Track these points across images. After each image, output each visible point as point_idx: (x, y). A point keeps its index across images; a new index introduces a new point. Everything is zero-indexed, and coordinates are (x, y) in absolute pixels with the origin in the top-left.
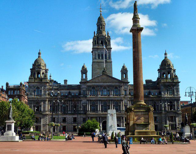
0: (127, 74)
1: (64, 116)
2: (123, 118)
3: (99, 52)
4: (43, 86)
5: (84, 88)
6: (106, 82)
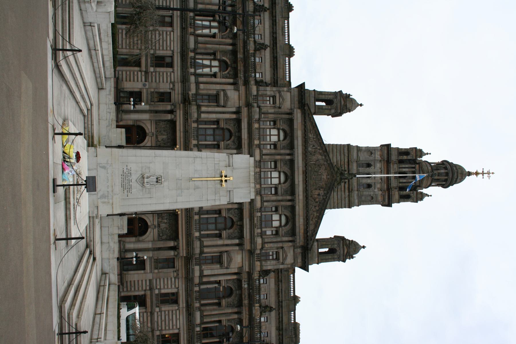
0: (333, 260)
2: (174, 248)
3: (378, 165)
5: (283, 99)
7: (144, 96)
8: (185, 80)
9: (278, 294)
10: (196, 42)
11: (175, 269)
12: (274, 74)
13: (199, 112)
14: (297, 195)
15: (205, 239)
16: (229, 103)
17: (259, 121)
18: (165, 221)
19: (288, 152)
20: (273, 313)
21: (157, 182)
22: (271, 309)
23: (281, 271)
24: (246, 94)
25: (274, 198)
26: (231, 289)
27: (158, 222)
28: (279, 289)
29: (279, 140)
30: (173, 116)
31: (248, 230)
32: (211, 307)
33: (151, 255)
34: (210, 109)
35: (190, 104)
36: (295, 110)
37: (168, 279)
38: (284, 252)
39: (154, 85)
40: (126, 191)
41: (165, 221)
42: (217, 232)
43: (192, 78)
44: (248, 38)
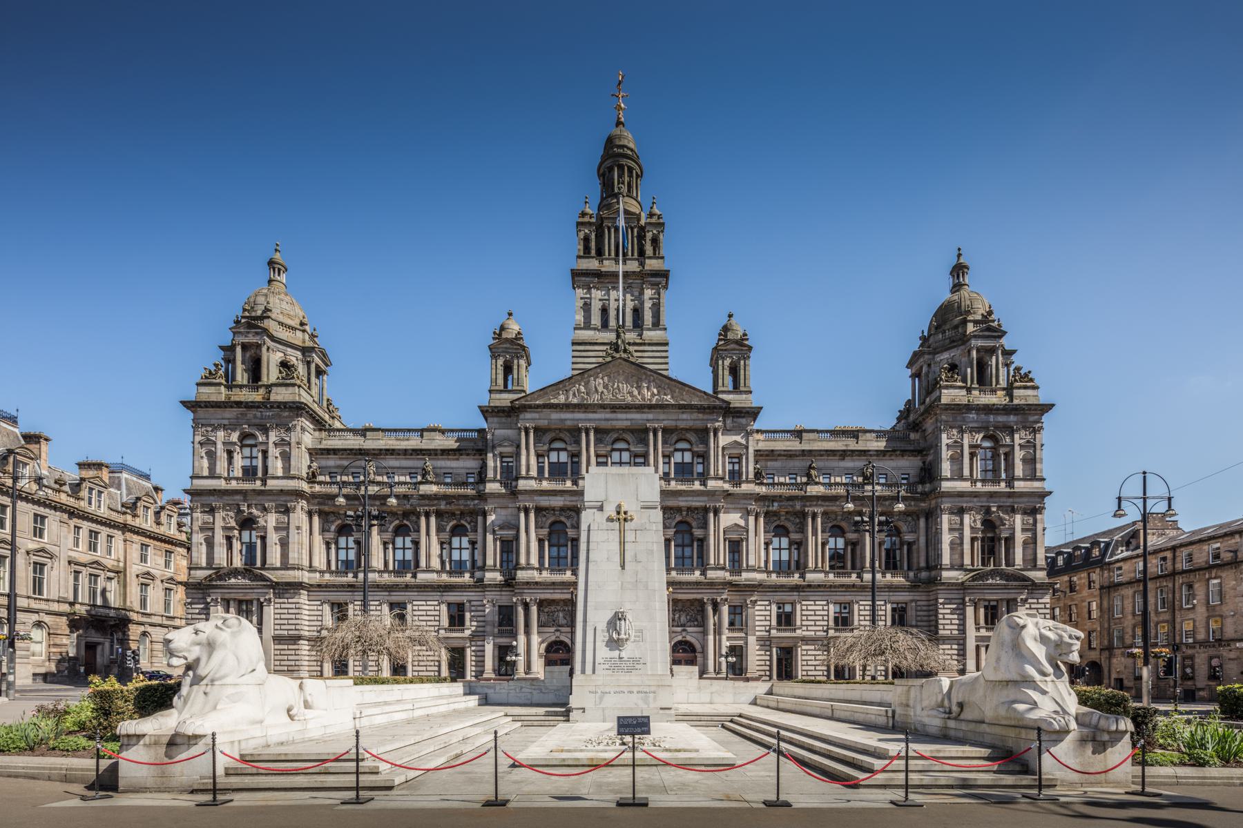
7: (503, 641)
29: (565, 449)
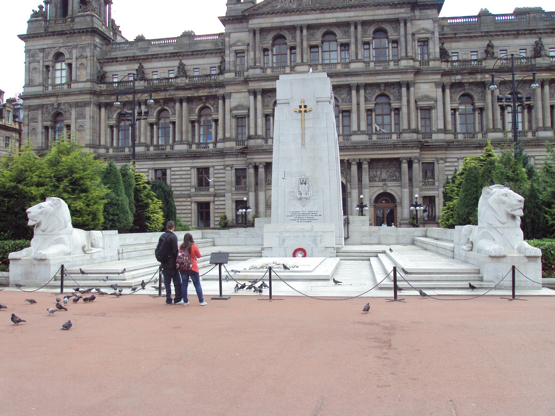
1: (161, 164)
2: (410, 163)
4: (76, 47)
5: (239, 41)
6: (333, 9)
7: (239, 197)
8: (222, 154)
9: (471, 37)
10: (181, 142)
11: (436, 162)
12: (211, 53)
13: (256, 137)
14: (349, 19)
15: (401, 127)
16: (245, 103)
17: (263, 69)
18: (379, 173)
19: (298, 32)
20: (496, 43)
21: (305, 184)
22: (490, 46)
23: (443, 35)
24: (234, 84)
25: (353, 47)
26: (463, 95)
27: (380, 181)
28: (465, 37)
30: (261, 166)
31: (391, 77)
32: (484, 119)
33: (418, 189)
34: (252, 125)
35: (247, 148)
36: (250, 26)
37: (446, 171)
38: (418, 32)
39: (228, 187)
40: (315, 218)
41: (379, 173)
42: (393, 113)
43: (220, 145)
44: (172, 85)
